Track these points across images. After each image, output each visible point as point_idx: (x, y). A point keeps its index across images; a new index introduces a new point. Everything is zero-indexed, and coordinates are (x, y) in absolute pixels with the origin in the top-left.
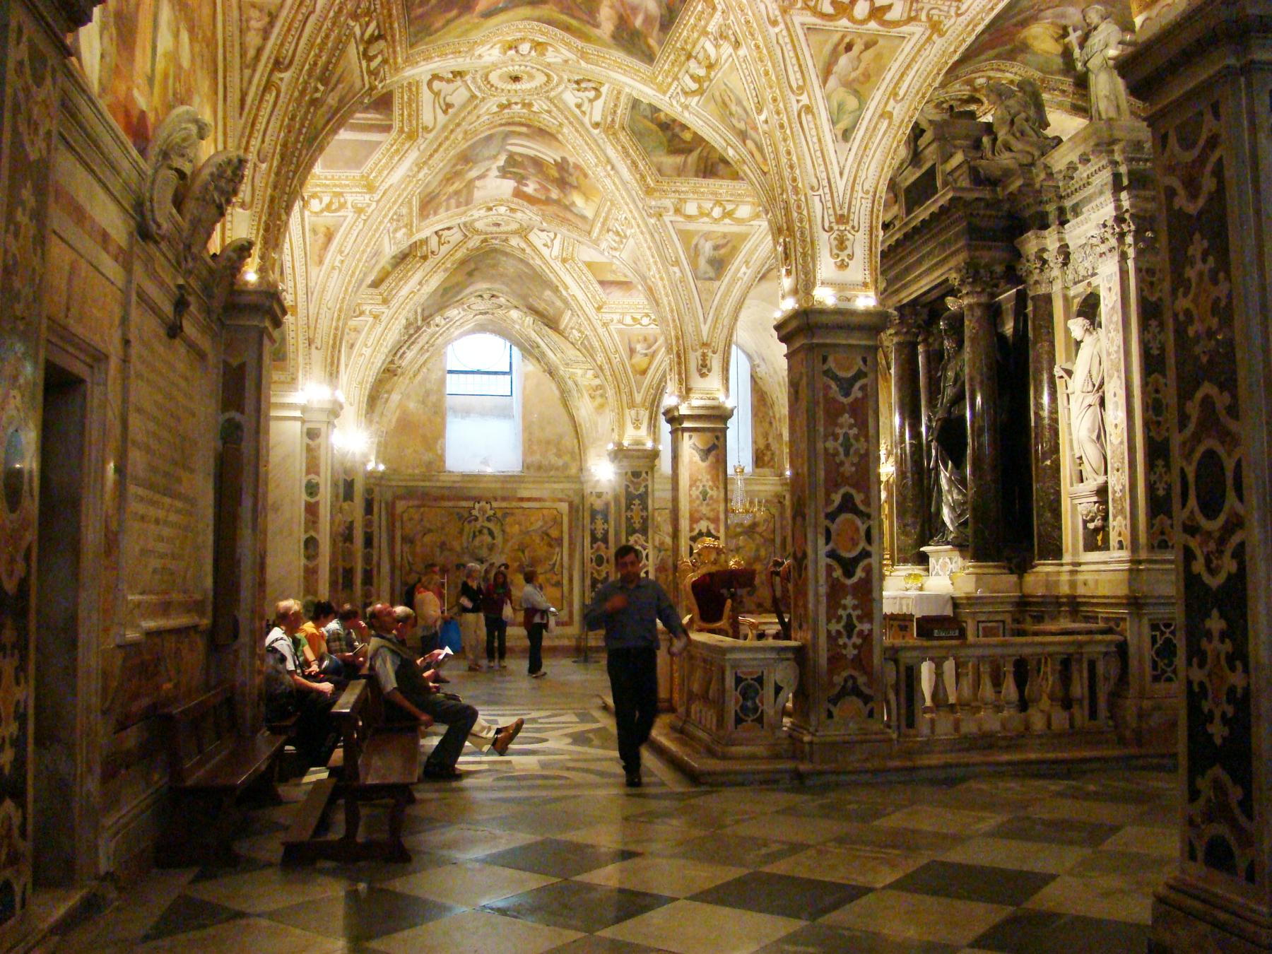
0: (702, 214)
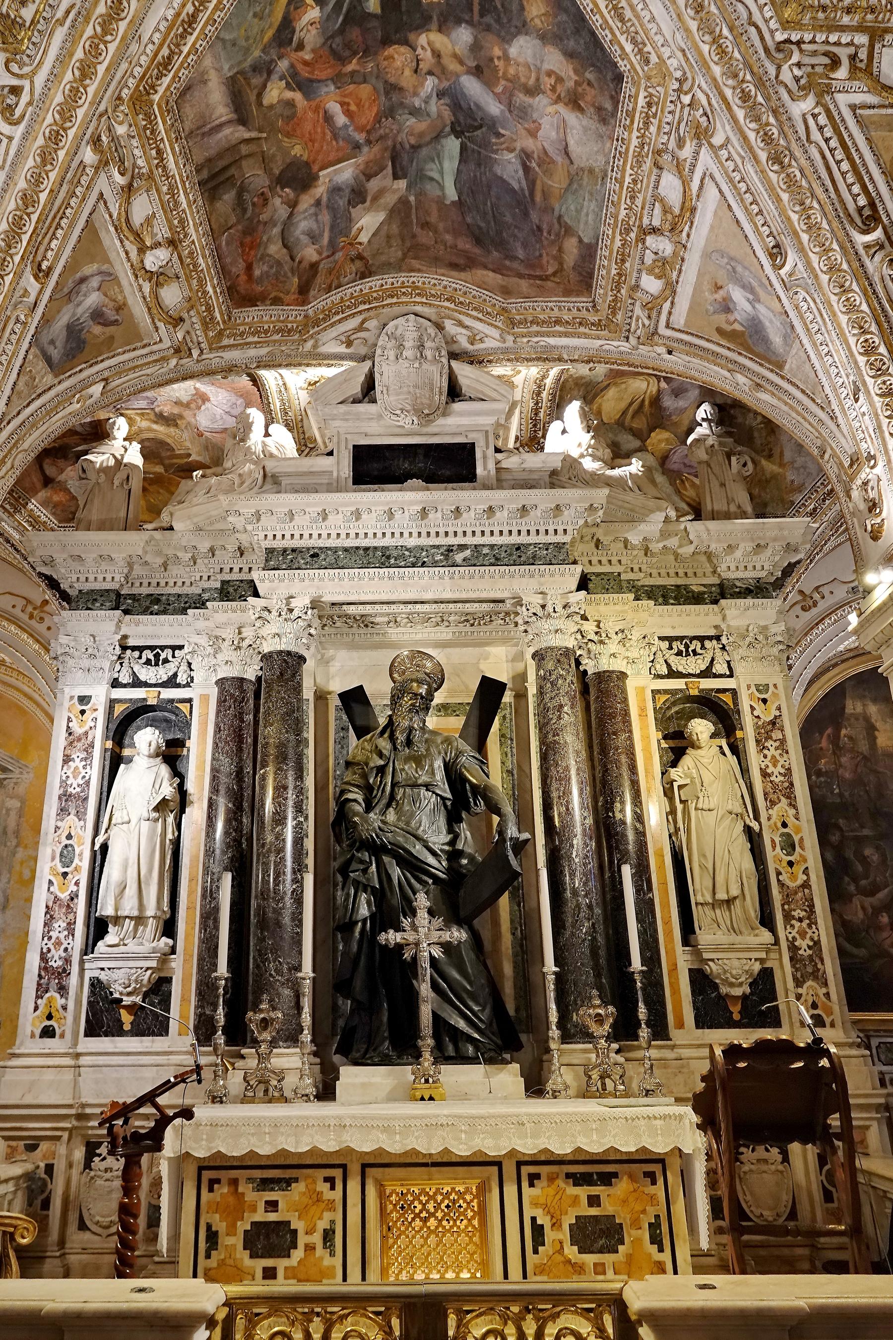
0: (138, 236)
